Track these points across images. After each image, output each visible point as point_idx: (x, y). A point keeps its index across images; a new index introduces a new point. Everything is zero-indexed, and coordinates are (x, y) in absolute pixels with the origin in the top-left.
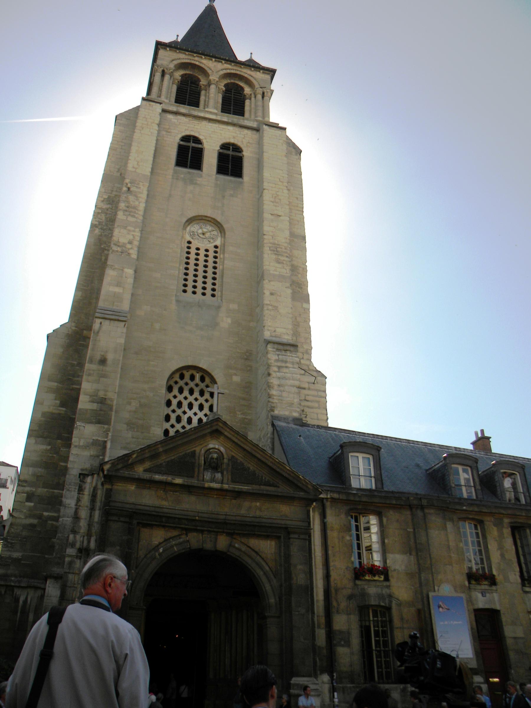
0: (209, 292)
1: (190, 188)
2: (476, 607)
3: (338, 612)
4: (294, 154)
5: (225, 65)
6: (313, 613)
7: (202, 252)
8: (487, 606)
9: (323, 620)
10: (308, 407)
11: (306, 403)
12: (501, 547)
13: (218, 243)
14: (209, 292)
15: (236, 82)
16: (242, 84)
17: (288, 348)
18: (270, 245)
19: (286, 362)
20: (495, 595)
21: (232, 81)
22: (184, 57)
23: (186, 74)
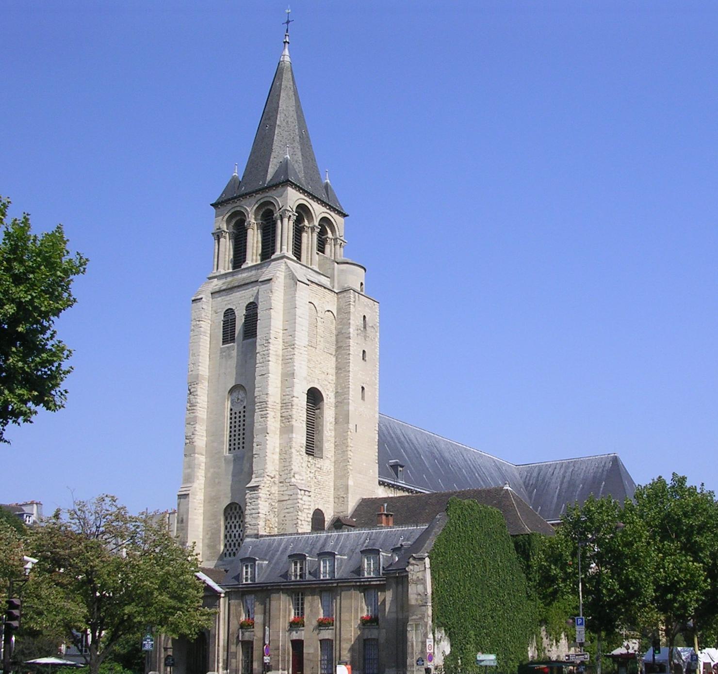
0: (241, 445)
1: (229, 362)
2: (292, 639)
3: (233, 644)
4: (292, 286)
5: (257, 196)
6: (218, 646)
7: (238, 415)
8: (297, 638)
9: (226, 648)
10: (288, 513)
11: (287, 511)
12: (311, 606)
13: (245, 404)
14: (241, 445)
15: (268, 207)
16: (271, 208)
17: (254, 489)
18: (258, 404)
19: (253, 498)
20: (303, 632)
21: (266, 208)
22: (228, 210)
23: (237, 221)
